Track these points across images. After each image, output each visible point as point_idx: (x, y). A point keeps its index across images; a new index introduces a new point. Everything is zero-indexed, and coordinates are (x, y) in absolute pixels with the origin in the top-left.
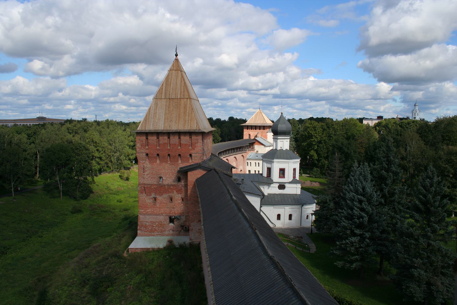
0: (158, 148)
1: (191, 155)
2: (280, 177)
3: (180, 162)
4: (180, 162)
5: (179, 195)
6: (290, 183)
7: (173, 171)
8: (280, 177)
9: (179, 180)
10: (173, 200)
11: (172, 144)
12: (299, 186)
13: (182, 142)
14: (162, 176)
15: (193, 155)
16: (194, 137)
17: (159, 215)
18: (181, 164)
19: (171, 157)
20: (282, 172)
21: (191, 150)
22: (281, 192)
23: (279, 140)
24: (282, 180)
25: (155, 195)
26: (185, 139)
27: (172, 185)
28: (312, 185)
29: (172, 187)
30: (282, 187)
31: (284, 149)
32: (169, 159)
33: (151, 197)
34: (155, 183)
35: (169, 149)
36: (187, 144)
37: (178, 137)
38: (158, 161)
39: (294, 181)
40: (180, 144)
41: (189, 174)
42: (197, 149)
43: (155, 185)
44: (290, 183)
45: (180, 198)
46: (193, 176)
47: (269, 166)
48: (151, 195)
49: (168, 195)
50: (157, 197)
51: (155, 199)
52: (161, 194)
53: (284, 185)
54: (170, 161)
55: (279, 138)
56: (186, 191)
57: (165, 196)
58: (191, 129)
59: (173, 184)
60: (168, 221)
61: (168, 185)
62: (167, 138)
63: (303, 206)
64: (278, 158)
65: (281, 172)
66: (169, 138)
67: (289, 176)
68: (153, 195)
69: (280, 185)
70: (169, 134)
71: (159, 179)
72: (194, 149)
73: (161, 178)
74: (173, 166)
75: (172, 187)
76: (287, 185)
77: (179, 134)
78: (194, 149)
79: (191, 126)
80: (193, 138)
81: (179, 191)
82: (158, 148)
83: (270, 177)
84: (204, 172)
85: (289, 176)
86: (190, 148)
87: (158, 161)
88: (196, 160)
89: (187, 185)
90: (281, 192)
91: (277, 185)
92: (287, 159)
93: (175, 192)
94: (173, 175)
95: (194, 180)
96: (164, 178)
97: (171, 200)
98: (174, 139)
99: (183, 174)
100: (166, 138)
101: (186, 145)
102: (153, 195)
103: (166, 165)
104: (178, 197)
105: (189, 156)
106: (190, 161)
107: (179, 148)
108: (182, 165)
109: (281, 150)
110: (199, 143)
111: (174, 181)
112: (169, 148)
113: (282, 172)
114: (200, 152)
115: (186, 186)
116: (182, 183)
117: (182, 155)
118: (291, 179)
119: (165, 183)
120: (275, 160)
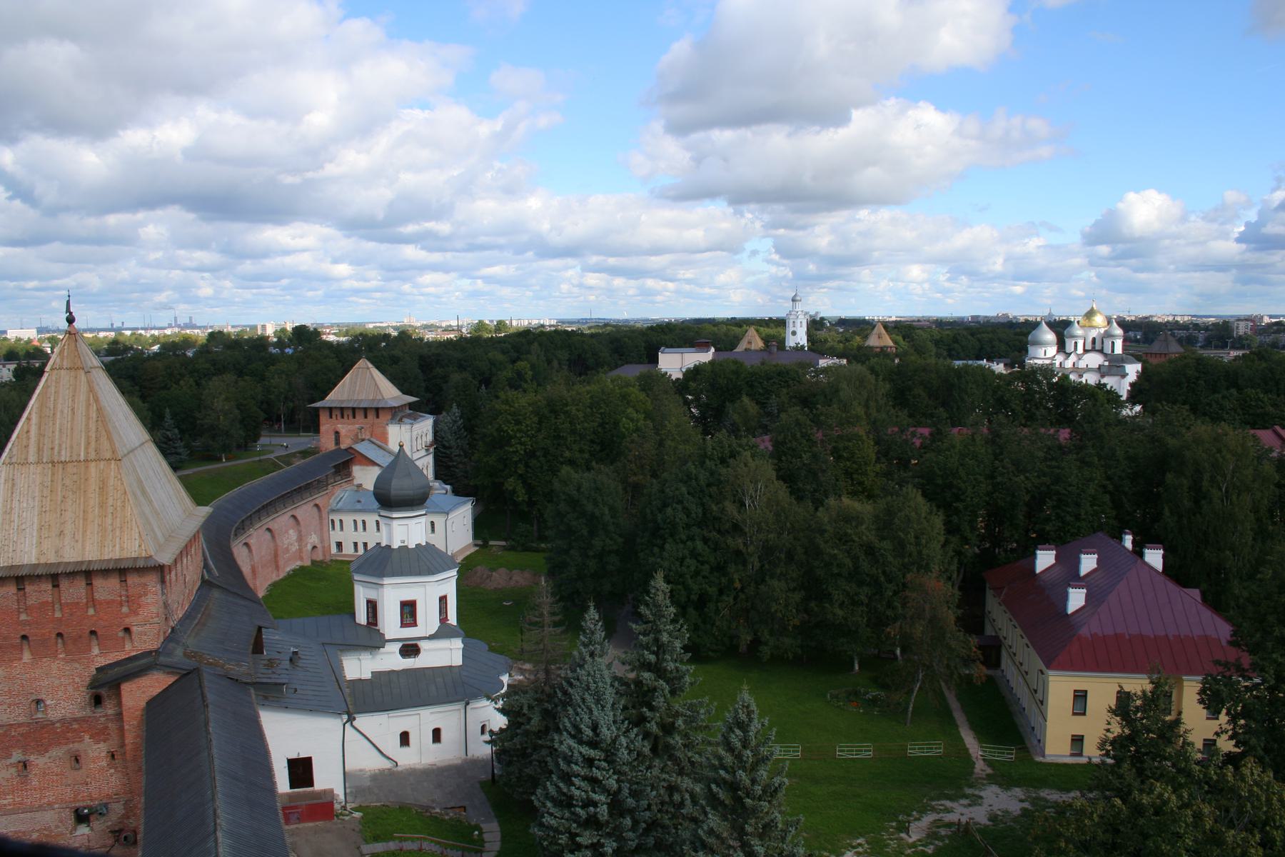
0: (23, 617)
1: (127, 630)
2: (403, 625)
3: (96, 651)
4: (96, 651)
5: (102, 745)
6: (431, 637)
7: (77, 680)
8: (403, 625)
9: (97, 701)
10: (82, 761)
11: (67, 604)
12: (457, 644)
13: (97, 596)
14: (44, 697)
15: (134, 629)
16: (133, 580)
17: (41, 808)
18: (99, 657)
19: (66, 640)
20: (409, 611)
21: (127, 616)
22: (410, 663)
23: (395, 523)
24: (409, 633)
25: (24, 753)
26: (106, 589)
27: (75, 720)
28: (512, 583)
29: (76, 726)
30: (410, 649)
31: (412, 546)
32: (60, 645)
33: (9, 761)
34: (21, 719)
35: (60, 620)
36: (113, 601)
37: (84, 583)
38: (27, 656)
39: (444, 632)
40: (92, 601)
41: (126, 688)
42: (144, 613)
43: (20, 725)
44: (431, 637)
45: (103, 754)
46: (137, 694)
47: (372, 595)
48: (9, 756)
49: (65, 748)
50: (32, 758)
51: (25, 765)
52: (43, 749)
53: (416, 646)
54: (67, 653)
55: (395, 515)
56: (121, 730)
57: (56, 752)
58: (126, 555)
59: (78, 715)
60: (71, 821)
61: (62, 721)
62: (50, 586)
63: (467, 704)
64: (393, 575)
65: (407, 609)
66: (56, 586)
67: (428, 620)
68: (17, 756)
69: (404, 646)
70: (55, 577)
71: (33, 705)
72: (136, 613)
73: (38, 702)
74: (77, 665)
75: (76, 726)
76: (423, 645)
77: (88, 574)
78: (136, 613)
79: (122, 549)
80: (130, 581)
81: (100, 735)
82: (23, 617)
83: (376, 624)
84: (171, 679)
85: (428, 620)
86: (125, 609)
87: (27, 656)
88: (146, 638)
89: (121, 714)
90: (410, 663)
91: (399, 645)
92: (420, 574)
93: (87, 737)
94: (77, 689)
95: (143, 704)
96: (48, 702)
97: (77, 761)
98: (74, 591)
99: (104, 687)
100: (47, 586)
101: (109, 603)
102: (17, 756)
103: (54, 666)
104: (95, 752)
105: (121, 634)
106: (128, 647)
107: (91, 612)
108: (102, 662)
109: (404, 549)
110: (150, 596)
111: (83, 708)
112: (58, 615)
113: (409, 611)
114: (156, 620)
115: (119, 716)
116: (109, 709)
117: (99, 633)
118: (434, 626)
119: (54, 715)
120: (387, 581)
